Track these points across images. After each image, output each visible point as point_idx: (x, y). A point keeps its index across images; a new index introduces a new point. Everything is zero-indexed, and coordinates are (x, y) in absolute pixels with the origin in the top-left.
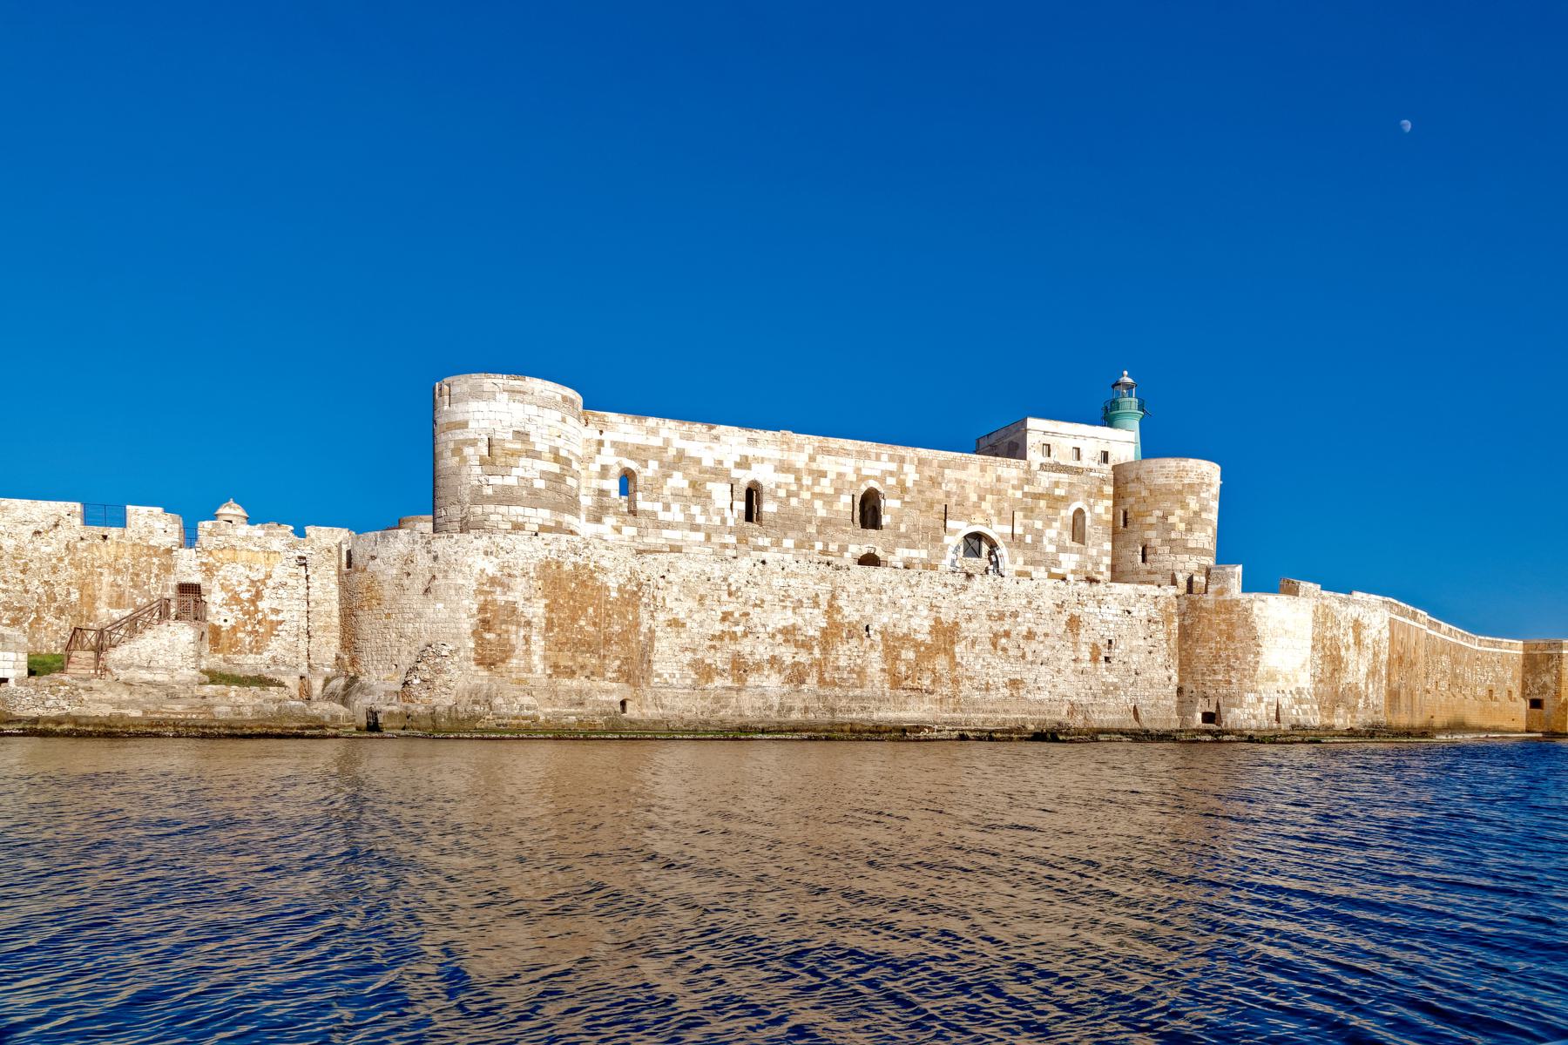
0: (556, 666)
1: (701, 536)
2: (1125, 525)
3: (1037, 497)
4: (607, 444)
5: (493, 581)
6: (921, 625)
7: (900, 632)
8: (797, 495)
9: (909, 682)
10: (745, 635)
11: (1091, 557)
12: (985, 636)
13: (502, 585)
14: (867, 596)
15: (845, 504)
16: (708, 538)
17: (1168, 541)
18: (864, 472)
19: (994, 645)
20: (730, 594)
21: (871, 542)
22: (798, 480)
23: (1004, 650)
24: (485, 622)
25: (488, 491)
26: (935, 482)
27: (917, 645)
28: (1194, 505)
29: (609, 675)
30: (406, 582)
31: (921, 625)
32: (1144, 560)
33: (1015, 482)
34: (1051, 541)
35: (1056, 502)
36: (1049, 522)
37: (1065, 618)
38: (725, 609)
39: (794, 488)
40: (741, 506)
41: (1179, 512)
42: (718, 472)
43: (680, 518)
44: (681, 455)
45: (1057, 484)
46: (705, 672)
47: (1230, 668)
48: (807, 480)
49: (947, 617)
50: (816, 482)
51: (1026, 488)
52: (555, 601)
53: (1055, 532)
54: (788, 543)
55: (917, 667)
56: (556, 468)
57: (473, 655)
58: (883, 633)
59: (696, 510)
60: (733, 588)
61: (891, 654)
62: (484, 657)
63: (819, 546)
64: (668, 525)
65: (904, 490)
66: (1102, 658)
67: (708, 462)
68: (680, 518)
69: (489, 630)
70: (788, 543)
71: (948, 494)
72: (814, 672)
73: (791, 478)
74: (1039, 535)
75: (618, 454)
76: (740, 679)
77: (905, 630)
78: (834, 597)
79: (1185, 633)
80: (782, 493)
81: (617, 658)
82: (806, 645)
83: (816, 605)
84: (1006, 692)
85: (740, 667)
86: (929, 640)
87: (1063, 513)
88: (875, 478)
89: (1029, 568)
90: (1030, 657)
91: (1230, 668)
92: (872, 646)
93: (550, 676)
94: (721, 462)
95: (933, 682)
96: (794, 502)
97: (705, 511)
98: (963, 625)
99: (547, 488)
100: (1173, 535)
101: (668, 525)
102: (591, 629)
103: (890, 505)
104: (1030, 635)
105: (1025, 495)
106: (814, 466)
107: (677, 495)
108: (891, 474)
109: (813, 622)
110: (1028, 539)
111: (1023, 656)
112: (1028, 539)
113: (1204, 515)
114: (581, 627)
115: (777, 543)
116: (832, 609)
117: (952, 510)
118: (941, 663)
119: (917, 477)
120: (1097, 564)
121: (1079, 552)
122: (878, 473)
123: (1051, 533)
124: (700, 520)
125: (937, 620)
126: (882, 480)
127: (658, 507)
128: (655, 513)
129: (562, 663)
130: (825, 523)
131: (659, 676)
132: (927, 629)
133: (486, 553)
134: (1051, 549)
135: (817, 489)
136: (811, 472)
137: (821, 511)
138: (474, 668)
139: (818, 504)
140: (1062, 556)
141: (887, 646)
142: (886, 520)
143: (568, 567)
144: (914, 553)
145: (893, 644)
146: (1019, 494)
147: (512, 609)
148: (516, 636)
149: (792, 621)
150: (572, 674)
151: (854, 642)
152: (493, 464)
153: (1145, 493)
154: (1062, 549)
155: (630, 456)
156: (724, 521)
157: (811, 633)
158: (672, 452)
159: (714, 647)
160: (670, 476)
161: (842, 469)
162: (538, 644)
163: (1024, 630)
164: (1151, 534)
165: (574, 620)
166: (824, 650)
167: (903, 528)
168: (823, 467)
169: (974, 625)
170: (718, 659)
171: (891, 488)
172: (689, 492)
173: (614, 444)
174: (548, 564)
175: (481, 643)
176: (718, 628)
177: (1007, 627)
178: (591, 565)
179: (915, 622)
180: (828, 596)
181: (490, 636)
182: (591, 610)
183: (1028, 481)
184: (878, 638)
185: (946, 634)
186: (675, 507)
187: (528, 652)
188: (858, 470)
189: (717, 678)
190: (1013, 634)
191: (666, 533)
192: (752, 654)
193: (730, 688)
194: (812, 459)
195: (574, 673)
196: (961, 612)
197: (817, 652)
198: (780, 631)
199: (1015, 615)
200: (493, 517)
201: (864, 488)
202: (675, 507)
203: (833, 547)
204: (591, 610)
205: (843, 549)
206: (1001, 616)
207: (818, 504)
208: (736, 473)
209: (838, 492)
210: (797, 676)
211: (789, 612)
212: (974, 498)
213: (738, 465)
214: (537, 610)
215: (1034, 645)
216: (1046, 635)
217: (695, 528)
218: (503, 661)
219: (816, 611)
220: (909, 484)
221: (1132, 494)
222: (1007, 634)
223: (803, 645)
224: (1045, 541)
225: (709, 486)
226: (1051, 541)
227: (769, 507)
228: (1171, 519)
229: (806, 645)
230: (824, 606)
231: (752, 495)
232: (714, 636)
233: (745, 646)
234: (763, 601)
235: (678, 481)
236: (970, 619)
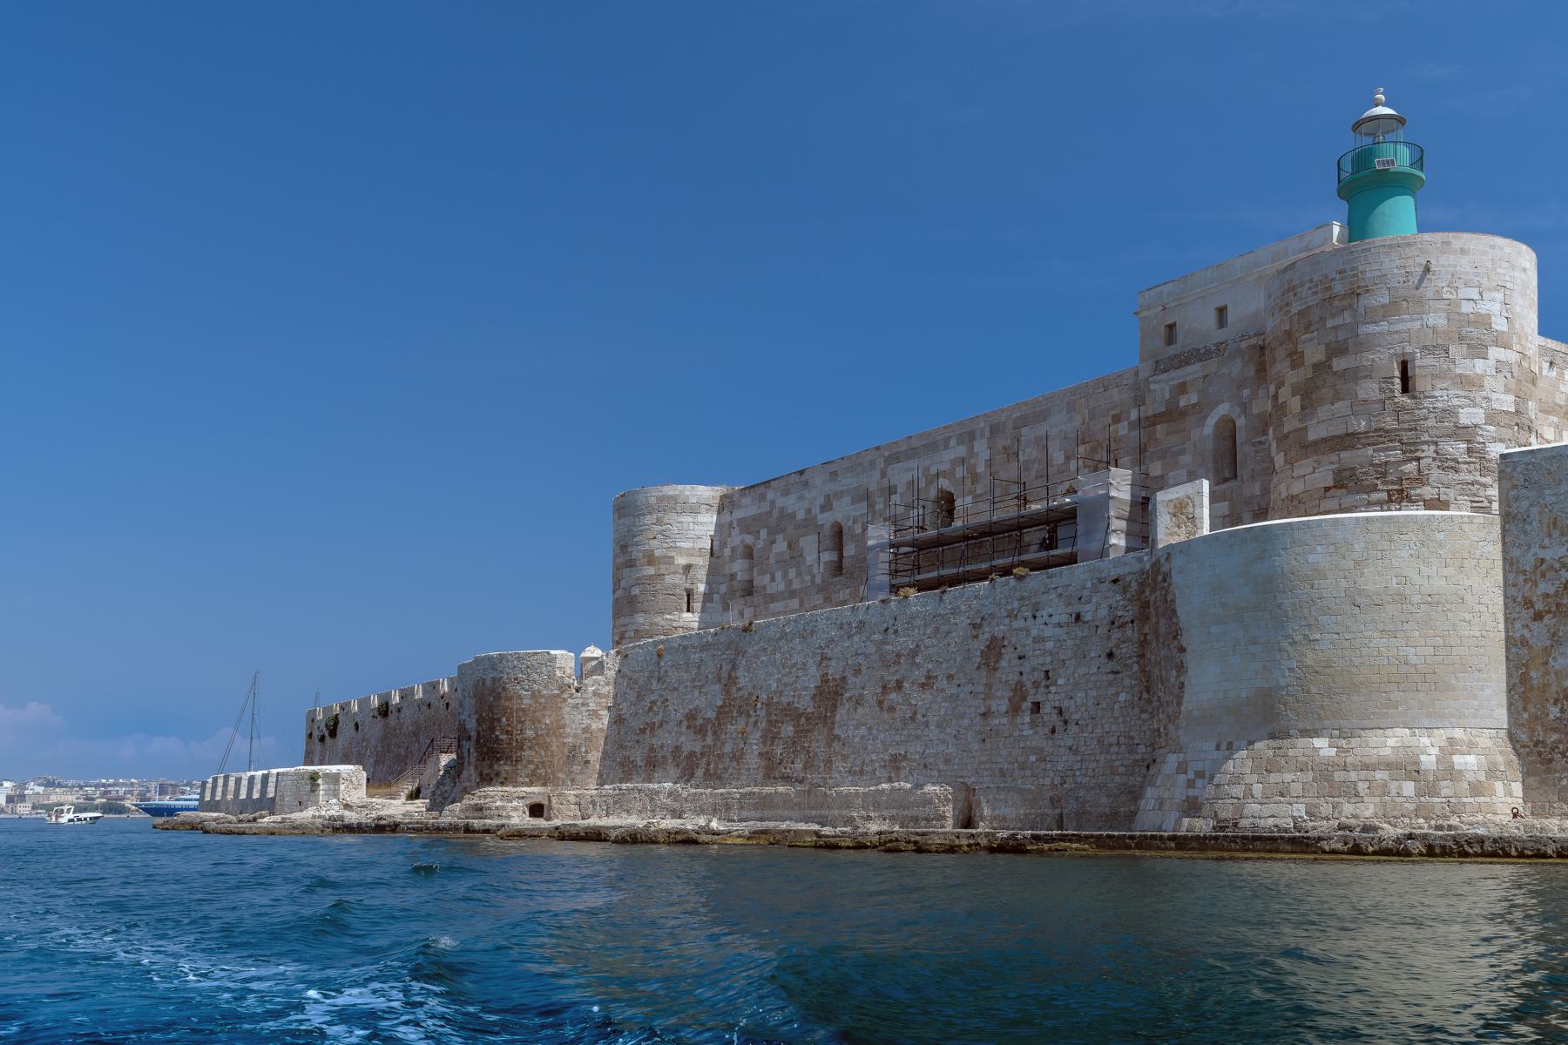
3: (1154, 420)
19: (880, 703)
28: (1314, 353)
42: (809, 524)
45: (1182, 388)
49: (834, 670)
61: (770, 736)
82: (701, 731)
98: (851, 679)
113: (1339, 364)
125: (825, 680)
127: (766, 579)
163: (919, 675)
217: (793, 594)
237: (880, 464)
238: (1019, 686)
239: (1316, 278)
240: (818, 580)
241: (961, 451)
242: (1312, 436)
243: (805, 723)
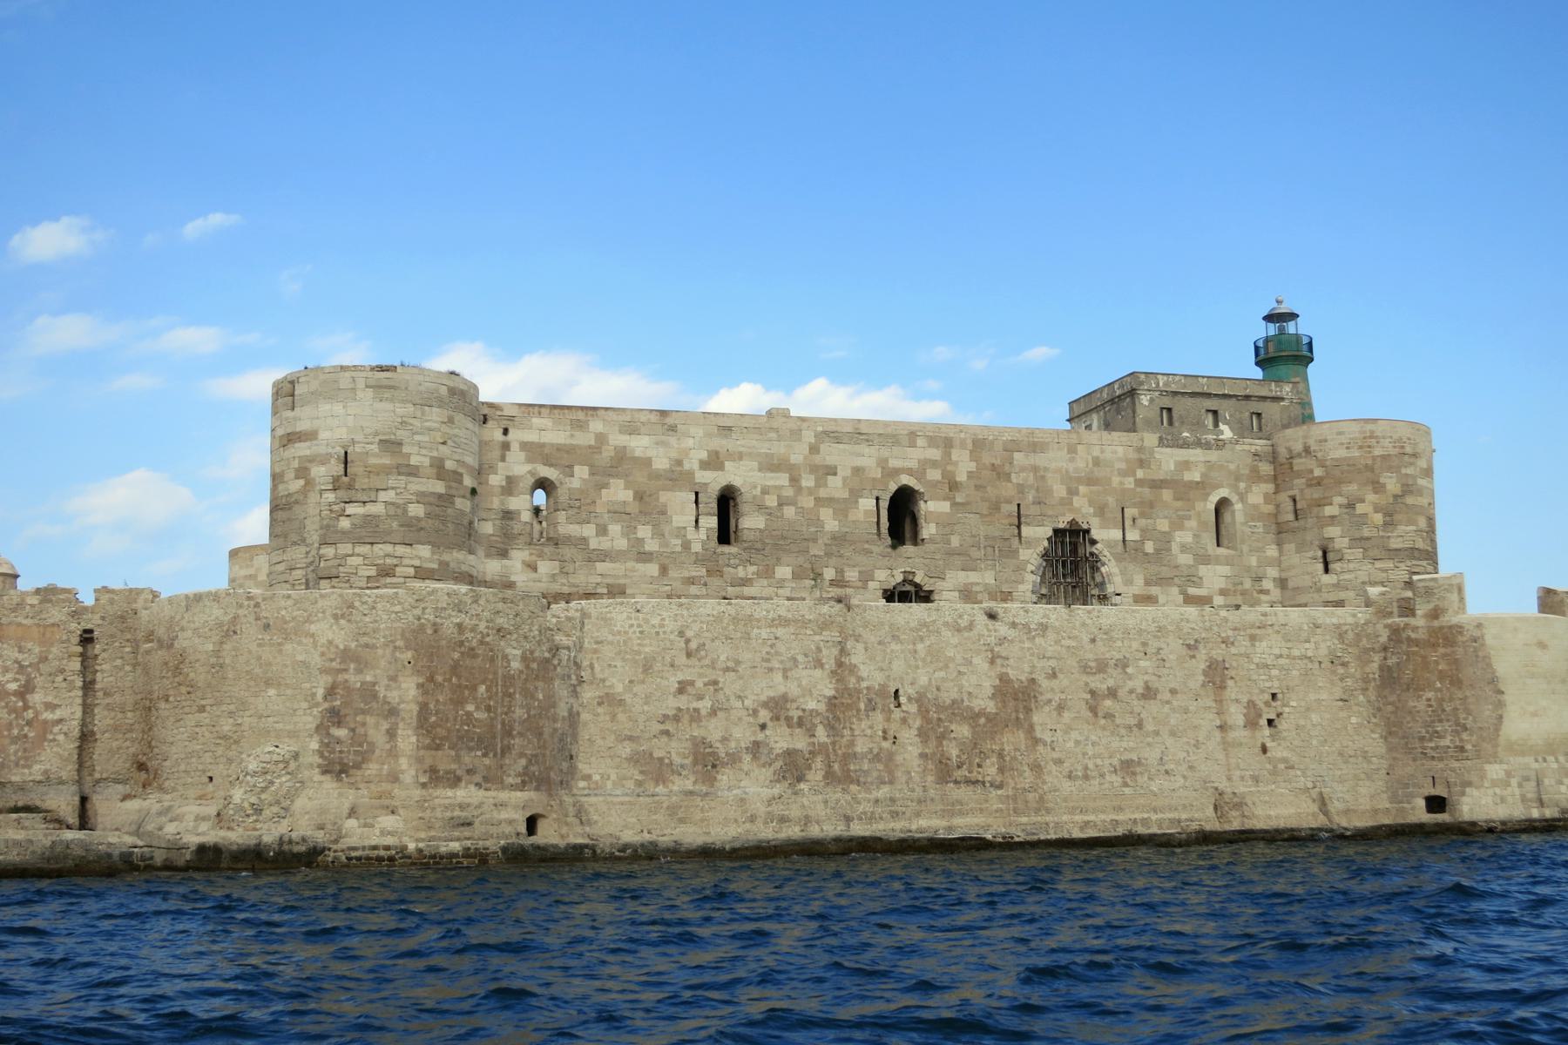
0: (433, 771)
1: (653, 569)
3: (1157, 485)
4: (515, 447)
5: (346, 655)
6: (979, 688)
7: (947, 697)
8: (791, 502)
9: (964, 772)
10: (713, 712)
11: (1248, 569)
12: (1079, 699)
13: (357, 659)
14: (895, 647)
15: (868, 510)
16: (664, 570)
17: (1357, 541)
18: (893, 463)
19: (1093, 710)
20: (689, 655)
21: (910, 562)
22: (794, 481)
23: (1109, 716)
25: (345, 523)
26: (1000, 473)
27: (973, 717)
28: (1392, 484)
29: (510, 780)
31: (979, 688)
32: (1327, 570)
33: (1123, 466)
34: (1184, 548)
35: (1186, 491)
36: (1178, 525)
37: (1201, 664)
38: (681, 677)
39: (789, 492)
40: (712, 522)
41: (1371, 497)
42: (677, 477)
43: (622, 544)
44: (622, 456)
46: (659, 770)
48: (808, 481)
50: (821, 483)
51: (1140, 474)
52: (431, 679)
53: (1190, 535)
54: (783, 572)
55: (974, 748)
56: (439, 487)
57: (317, 760)
58: (920, 699)
59: (644, 532)
60: (693, 645)
61: (933, 731)
62: (331, 762)
63: (829, 574)
64: (605, 556)
65: (954, 486)
66: (1264, 722)
67: (661, 463)
68: (622, 544)
69: (339, 724)
70: (783, 572)
71: (1021, 489)
72: (818, 763)
73: (782, 479)
74: (1165, 541)
75: (529, 460)
76: (711, 780)
77: (954, 695)
78: (843, 651)
80: (771, 501)
81: (522, 755)
82: (803, 723)
83: (819, 664)
84: (1117, 780)
85: (708, 762)
86: (991, 707)
87: (1199, 506)
88: (910, 472)
89: (1154, 590)
90: (1149, 727)
92: (904, 721)
93: (424, 785)
94: (679, 463)
95: (1001, 770)
96: (789, 512)
97: (659, 534)
98: (1045, 683)
99: (428, 515)
100: (1366, 532)
101: (605, 556)
102: (481, 715)
103: (931, 508)
104: (1149, 693)
105: (1139, 483)
106: (817, 459)
107: (618, 512)
108: (934, 464)
109: (813, 690)
110: (1149, 547)
111: (1140, 725)
112: (1149, 547)
113: (1410, 500)
114: (469, 714)
115: (768, 573)
116: (842, 669)
117: (1029, 510)
118: (1012, 740)
119: (972, 466)
120: (1258, 579)
121: (1228, 562)
122: (913, 464)
123: (1183, 537)
124: (651, 546)
125: (1004, 678)
126: (919, 474)
127: (589, 531)
128: (585, 540)
129: (443, 767)
130: (839, 539)
131: (588, 778)
132: (990, 692)
133: (336, 617)
134: (1185, 559)
135: (823, 493)
136: (814, 469)
137: (831, 524)
138: (318, 777)
139: (826, 514)
140: (1203, 570)
141: (927, 720)
142: (928, 530)
143: (448, 628)
144: (973, 577)
145: (935, 718)
146: (1129, 483)
147: (369, 692)
148: (376, 731)
149: (782, 689)
150: (455, 781)
151: (878, 717)
152: (350, 487)
153: (1318, 472)
154: (1205, 559)
155: (548, 462)
156: (686, 545)
157: (812, 705)
158: (608, 453)
159: (667, 733)
160: (606, 486)
161: (859, 462)
162: (408, 740)
163: (1138, 684)
164: (1333, 531)
165: (459, 702)
166: (830, 727)
167: (955, 541)
168: (831, 460)
169: (1063, 681)
170: (676, 750)
171: (934, 484)
172: (634, 508)
173: (525, 446)
174: (422, 628)
175: (328, 745)
176: (672, 704)
177: (1111, 683)
178: (482, 626)
179: (968, 683)
180: (835, 651)
181: (341, 733)
182: (482, 688)
183: (1142, 463)
184: (913, 708)
185: (1018, 698)
186: (615, 529)
187: (393, 753)
188: (882, 463)
189: (675, 778)
190: (1121, 693)
191: (601, 567)
192: (725, 740)
193: (691, 793)
194: (814, 449)
195: (459, 779)
196: (1040, 664)
197: (821, 734)
198: (765, 705)
199: (1123, 664)
200: (351, 561)
201: (893, 487)
202: (615, 529)
203: (852, 575)
204: (482, 688)
205: (866, 578)
206: (1102, 667)
207: (826, 514)
208: (703, 476)
209: (855, 494)
210: (793, 769)
211: (778, 677)
212: (1060, 491)
213: (705, 465)
214: (407, 692)
215: (1153, 707)
216: (1173, 692)
217: (645, 557)
218: (357, 766)
219: (818, 673)
220: (962, 477)
222: (1112, 693)
223: (800, 723)
224: (1175, 548)
225: (664, 497)
226: (1184, 548)
227: (749, 522)
228: (1360, 508)
229: (803, 723)
230: (830, 664)
231: (726, 502)
232: (666, 717)
233: (713, 730)
234: (738, 662)
235: (619, 492)
236: (1053, 675)
237: (809, 437)
238: (1251, 704)
239: (1395, 437)
240: (697, 547)
241: (935, 454)
242: (1395, 544)
243: (992, 725)
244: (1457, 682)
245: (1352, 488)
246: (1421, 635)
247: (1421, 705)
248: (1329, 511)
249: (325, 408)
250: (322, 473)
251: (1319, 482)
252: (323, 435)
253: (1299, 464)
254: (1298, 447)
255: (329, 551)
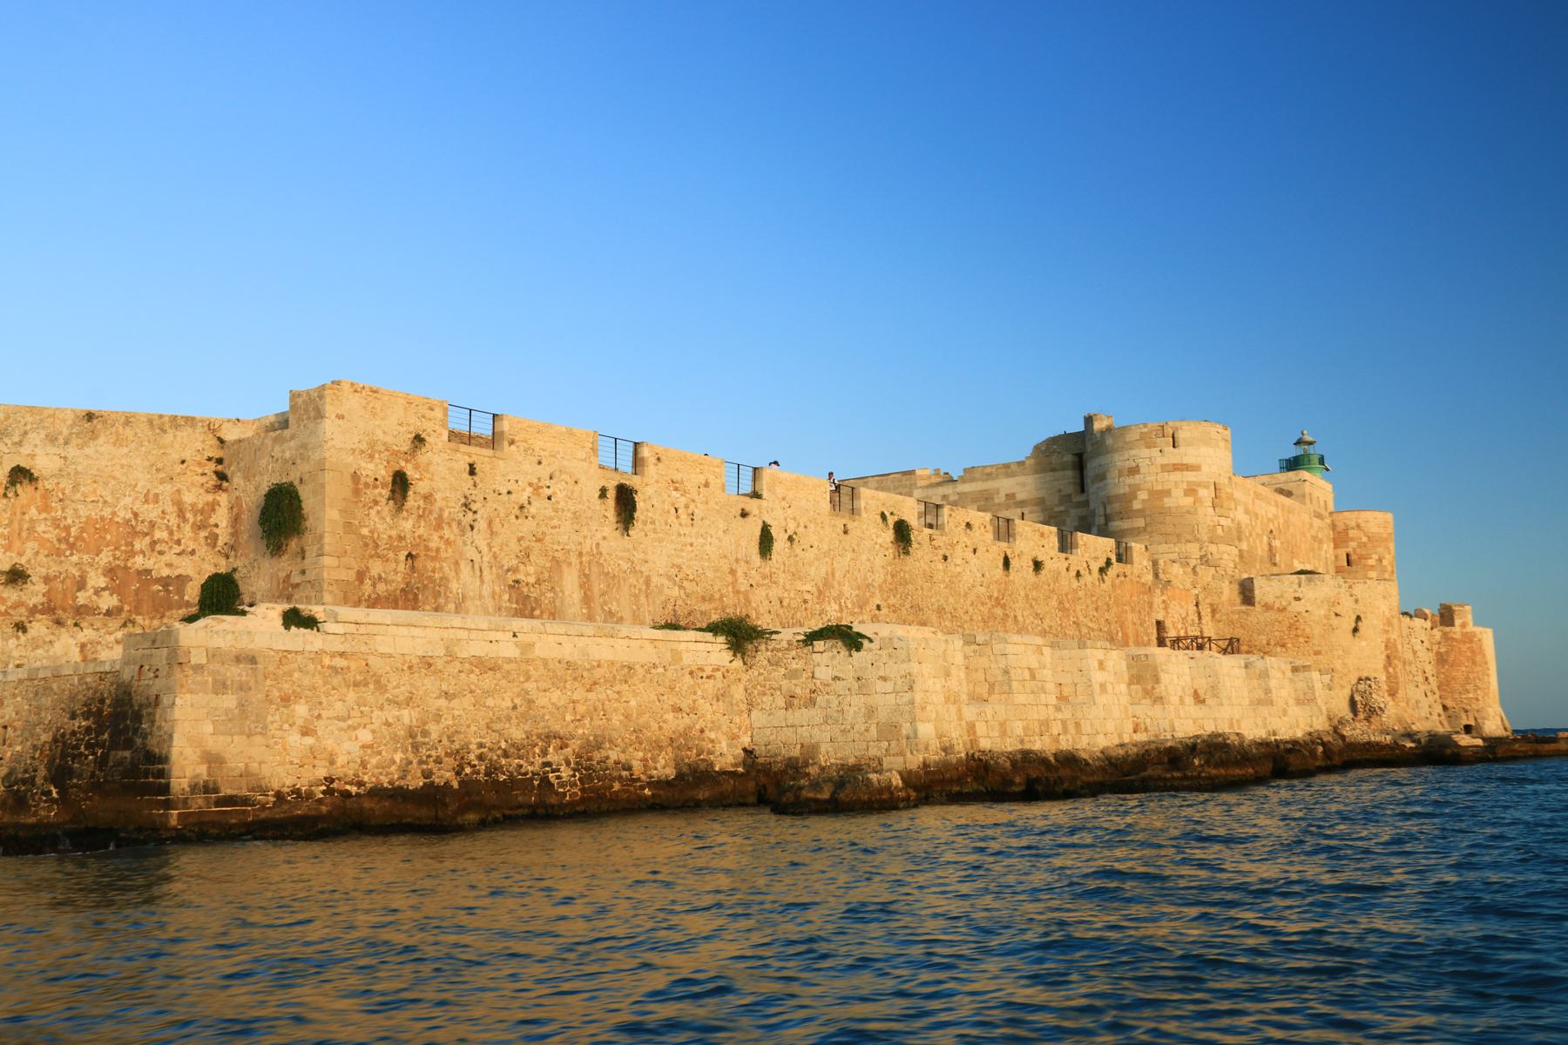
2: (1349, 564)
24: (1388, 657)
30: (1335, 621)
47: (1477, 688)
79: (1441, 660)
91: (1477, 688)
153: (1364, 539)
221: (1352, 540)
228: (1385, 562)
244: (1474, 663)
245: (1380, 550)
246: (1458, 636)
247: (1458, 674)
248: (1371, 562)
249: (1204, 450)
250: (1206, 494)
251: (1365, 545)
252: (1205, 468)
253: (1352, 533)
254: (1353, 524)
255: (1213, 548)
